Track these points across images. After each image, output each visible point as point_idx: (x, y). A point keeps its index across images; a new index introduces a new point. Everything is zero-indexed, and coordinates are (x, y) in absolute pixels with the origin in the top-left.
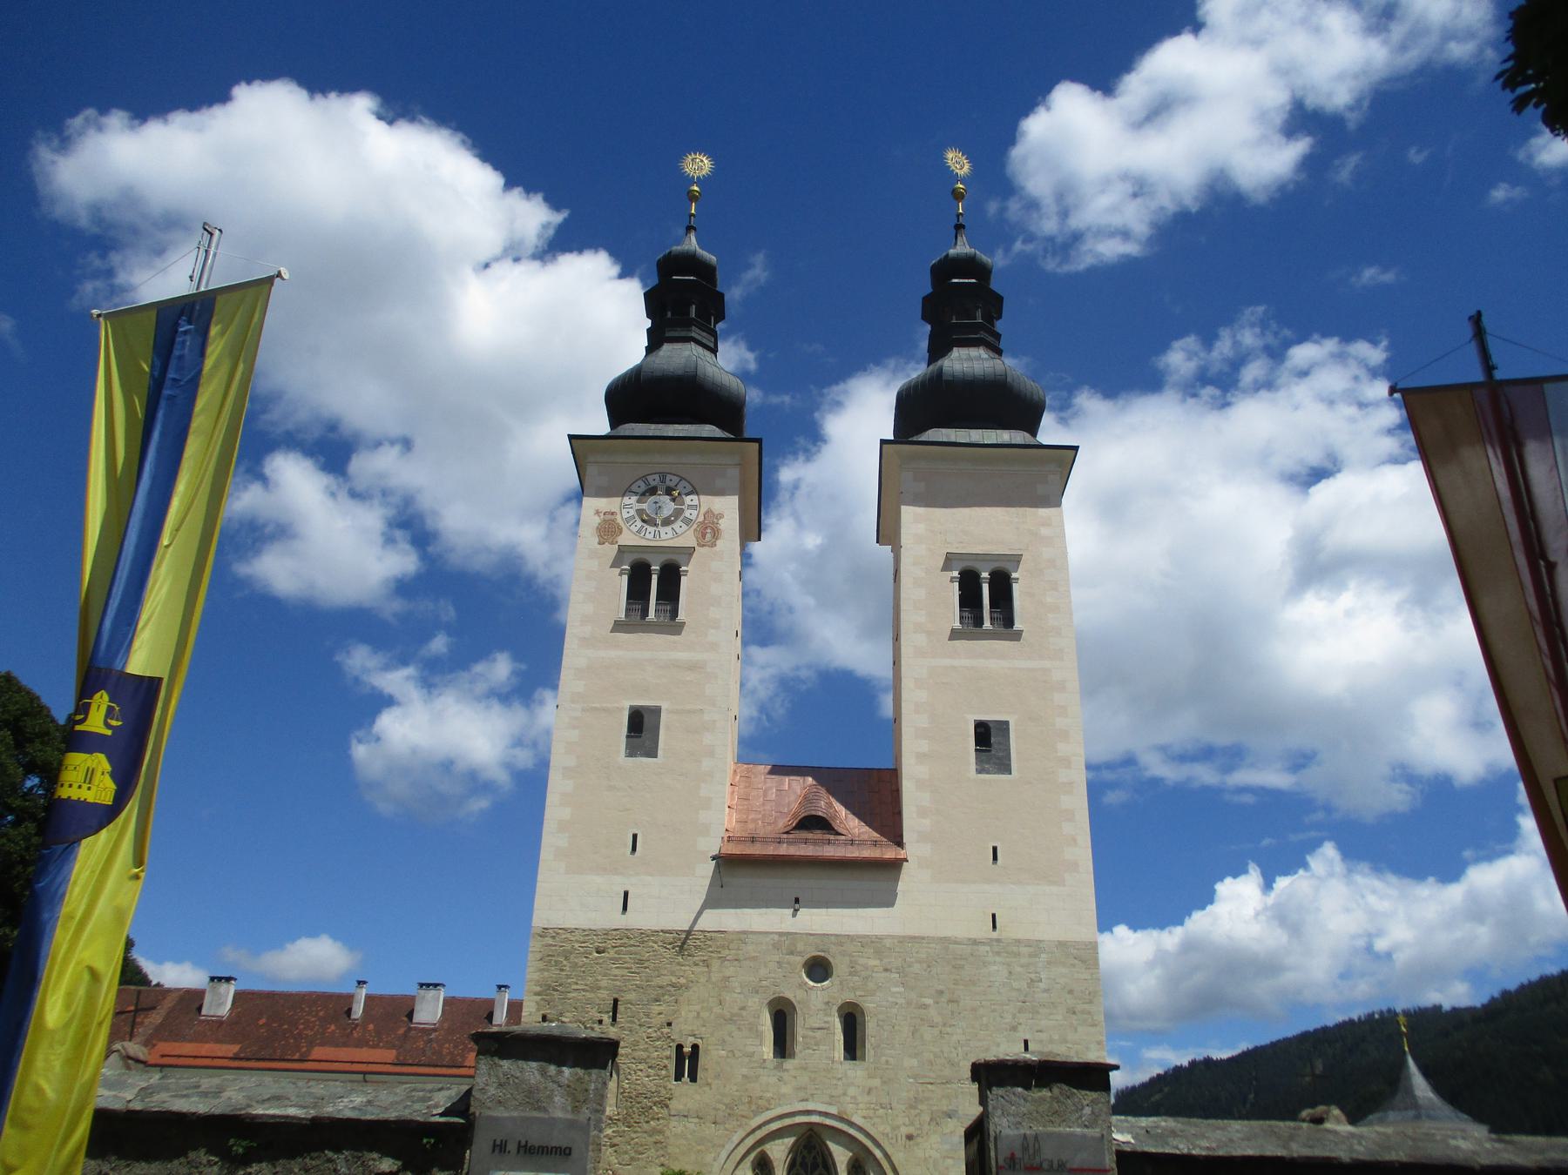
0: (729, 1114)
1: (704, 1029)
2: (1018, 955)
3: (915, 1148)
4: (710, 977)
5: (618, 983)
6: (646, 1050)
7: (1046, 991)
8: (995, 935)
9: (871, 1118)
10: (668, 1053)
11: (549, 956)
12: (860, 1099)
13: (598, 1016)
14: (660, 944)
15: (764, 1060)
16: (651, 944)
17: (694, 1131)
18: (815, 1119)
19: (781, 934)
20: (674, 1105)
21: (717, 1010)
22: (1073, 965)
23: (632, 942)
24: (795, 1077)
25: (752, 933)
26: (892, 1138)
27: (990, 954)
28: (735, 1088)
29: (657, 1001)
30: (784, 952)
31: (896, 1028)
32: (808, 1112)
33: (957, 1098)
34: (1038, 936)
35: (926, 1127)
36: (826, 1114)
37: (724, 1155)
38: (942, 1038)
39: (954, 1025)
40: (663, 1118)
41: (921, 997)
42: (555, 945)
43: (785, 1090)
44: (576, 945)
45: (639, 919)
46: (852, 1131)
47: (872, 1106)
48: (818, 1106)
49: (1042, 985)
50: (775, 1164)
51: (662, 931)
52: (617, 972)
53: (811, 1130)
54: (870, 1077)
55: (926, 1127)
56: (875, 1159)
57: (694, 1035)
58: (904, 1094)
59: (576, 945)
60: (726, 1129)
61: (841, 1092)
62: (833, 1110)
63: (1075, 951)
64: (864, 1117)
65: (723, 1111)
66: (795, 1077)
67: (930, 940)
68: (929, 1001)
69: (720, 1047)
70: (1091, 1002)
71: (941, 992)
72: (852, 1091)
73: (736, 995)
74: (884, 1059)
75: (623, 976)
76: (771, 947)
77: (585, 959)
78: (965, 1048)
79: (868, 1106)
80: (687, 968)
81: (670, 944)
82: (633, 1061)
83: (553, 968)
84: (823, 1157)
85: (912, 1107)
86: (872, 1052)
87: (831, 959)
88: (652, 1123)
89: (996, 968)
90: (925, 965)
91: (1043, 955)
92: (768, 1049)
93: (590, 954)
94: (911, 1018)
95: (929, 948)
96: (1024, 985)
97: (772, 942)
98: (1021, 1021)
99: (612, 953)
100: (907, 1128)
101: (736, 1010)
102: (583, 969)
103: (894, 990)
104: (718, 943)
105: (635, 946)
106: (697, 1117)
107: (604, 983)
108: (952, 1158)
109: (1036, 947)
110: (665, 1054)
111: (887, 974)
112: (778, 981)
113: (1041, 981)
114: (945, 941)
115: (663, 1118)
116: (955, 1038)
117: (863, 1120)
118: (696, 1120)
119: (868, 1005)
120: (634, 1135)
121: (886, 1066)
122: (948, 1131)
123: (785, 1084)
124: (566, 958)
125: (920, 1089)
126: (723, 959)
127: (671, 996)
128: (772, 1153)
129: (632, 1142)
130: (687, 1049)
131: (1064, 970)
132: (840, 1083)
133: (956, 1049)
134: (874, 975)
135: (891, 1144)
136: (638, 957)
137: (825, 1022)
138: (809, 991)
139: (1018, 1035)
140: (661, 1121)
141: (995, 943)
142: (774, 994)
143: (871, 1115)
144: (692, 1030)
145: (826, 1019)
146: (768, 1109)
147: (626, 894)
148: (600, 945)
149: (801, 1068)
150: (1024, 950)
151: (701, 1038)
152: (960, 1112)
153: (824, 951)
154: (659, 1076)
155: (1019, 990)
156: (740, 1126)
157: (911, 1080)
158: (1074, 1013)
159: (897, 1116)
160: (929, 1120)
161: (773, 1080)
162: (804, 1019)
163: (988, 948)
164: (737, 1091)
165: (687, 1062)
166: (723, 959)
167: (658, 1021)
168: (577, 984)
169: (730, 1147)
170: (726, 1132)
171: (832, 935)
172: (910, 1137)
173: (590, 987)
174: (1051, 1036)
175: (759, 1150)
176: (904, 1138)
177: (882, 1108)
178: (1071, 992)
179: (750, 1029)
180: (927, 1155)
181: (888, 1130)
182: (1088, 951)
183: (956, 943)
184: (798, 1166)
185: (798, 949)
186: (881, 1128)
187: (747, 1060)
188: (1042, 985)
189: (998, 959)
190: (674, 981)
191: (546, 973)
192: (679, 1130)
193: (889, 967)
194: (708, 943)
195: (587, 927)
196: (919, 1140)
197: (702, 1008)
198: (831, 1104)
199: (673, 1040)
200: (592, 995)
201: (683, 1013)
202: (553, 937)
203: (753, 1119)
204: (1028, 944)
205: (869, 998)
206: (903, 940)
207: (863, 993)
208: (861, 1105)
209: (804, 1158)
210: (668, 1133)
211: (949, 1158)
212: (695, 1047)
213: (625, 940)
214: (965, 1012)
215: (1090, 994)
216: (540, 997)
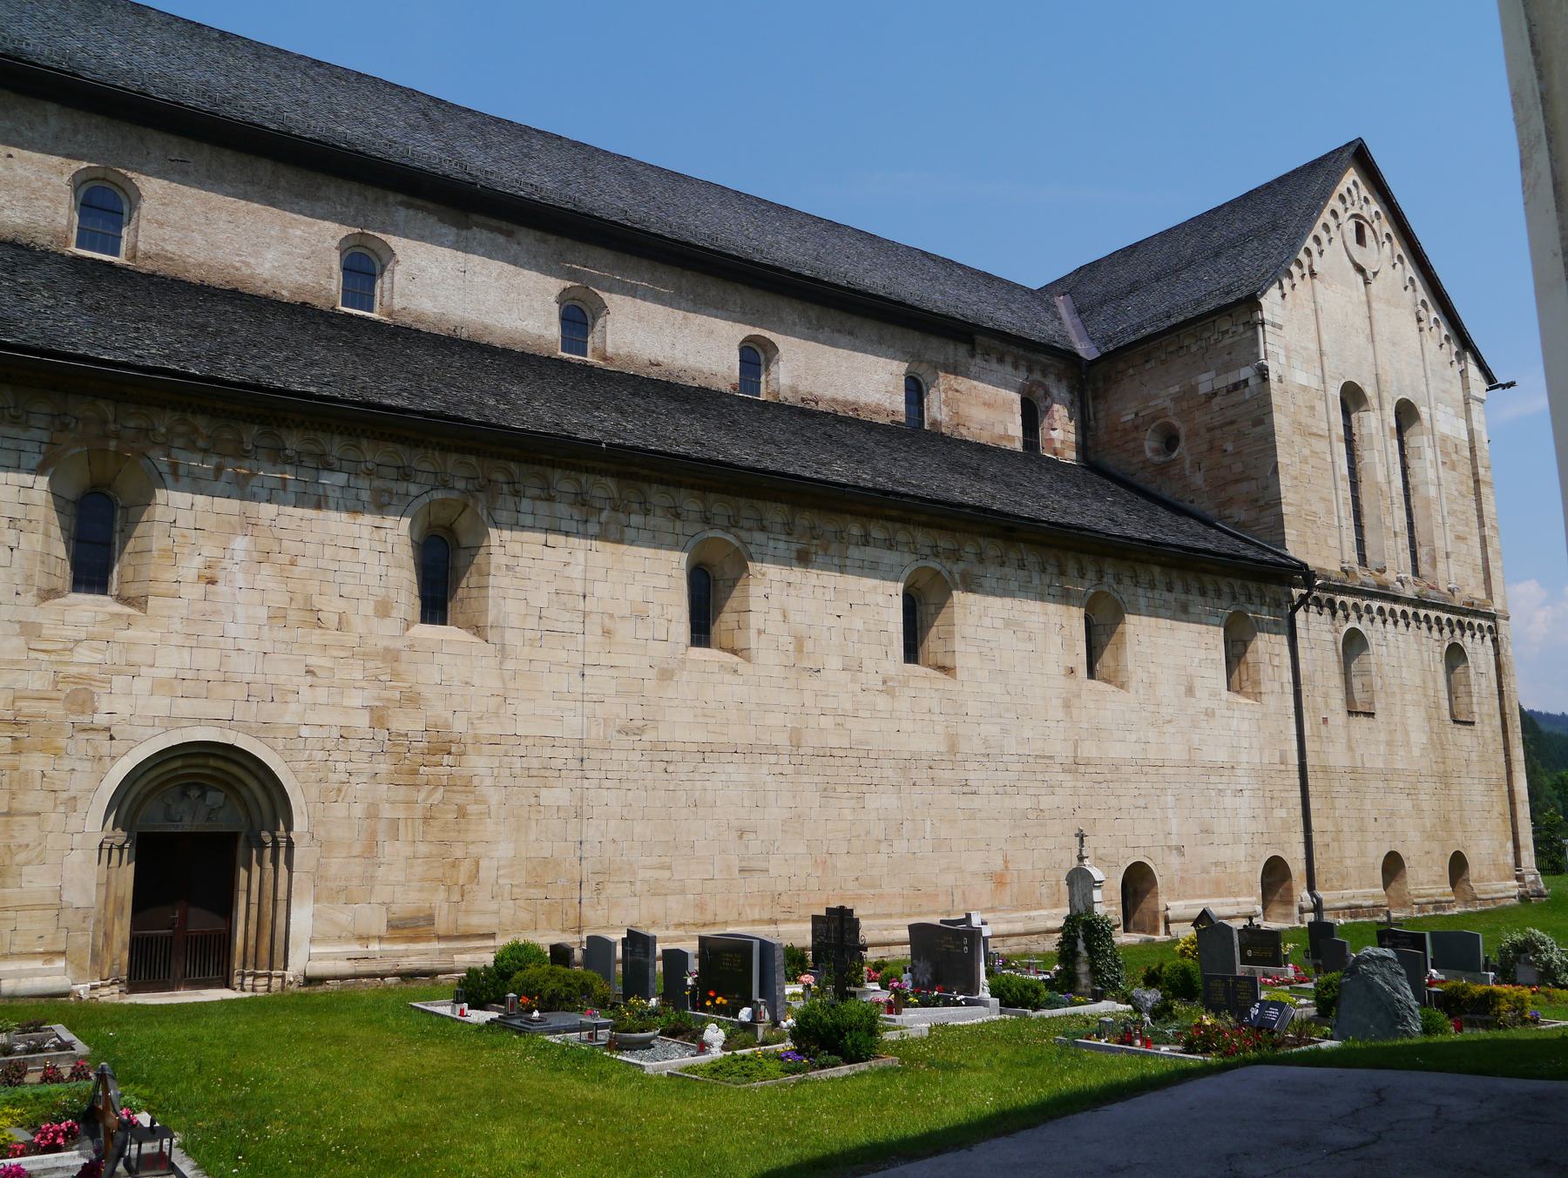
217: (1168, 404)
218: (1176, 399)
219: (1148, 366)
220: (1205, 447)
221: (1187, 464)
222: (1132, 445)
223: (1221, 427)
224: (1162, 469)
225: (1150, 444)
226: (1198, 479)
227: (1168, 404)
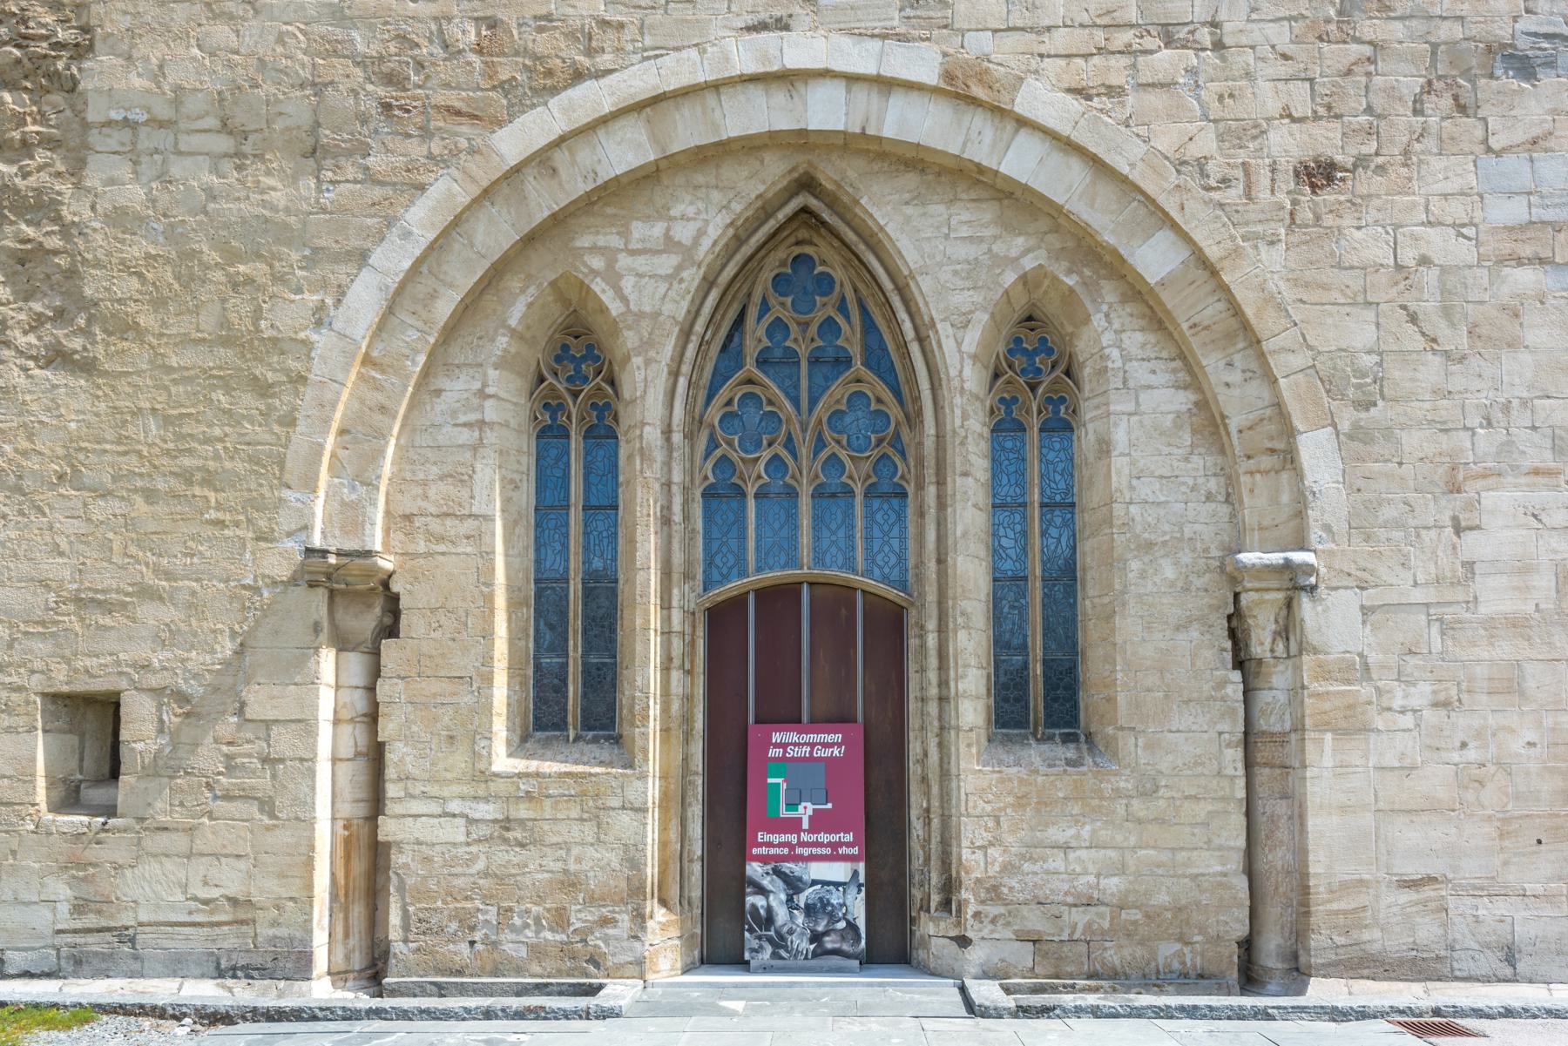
17: (211, 195)
26: (1225, 181)
32: (788, 78)
36: (885, 85)
47: (1122, 38)
50: (630, 339)
55: (1404, 119)
56: (1137, 292)
60: (370, 178)
62: (922, 65)
64: (1079, 92)
79: (1100, 36)
84: (869, 326)
106: (225, 127)
117: (1075, 104)
118: (224, 143)
122: (1520, 136)
128: (613, 278)
143: (1115, 80)
146: (578, 76)
170: (377, 193)
172: (1319, 174)
176: (1287, 182)
177: (1169, 42)
181: (1206, 143)
196: (1367, 182)
203: (500, 124)
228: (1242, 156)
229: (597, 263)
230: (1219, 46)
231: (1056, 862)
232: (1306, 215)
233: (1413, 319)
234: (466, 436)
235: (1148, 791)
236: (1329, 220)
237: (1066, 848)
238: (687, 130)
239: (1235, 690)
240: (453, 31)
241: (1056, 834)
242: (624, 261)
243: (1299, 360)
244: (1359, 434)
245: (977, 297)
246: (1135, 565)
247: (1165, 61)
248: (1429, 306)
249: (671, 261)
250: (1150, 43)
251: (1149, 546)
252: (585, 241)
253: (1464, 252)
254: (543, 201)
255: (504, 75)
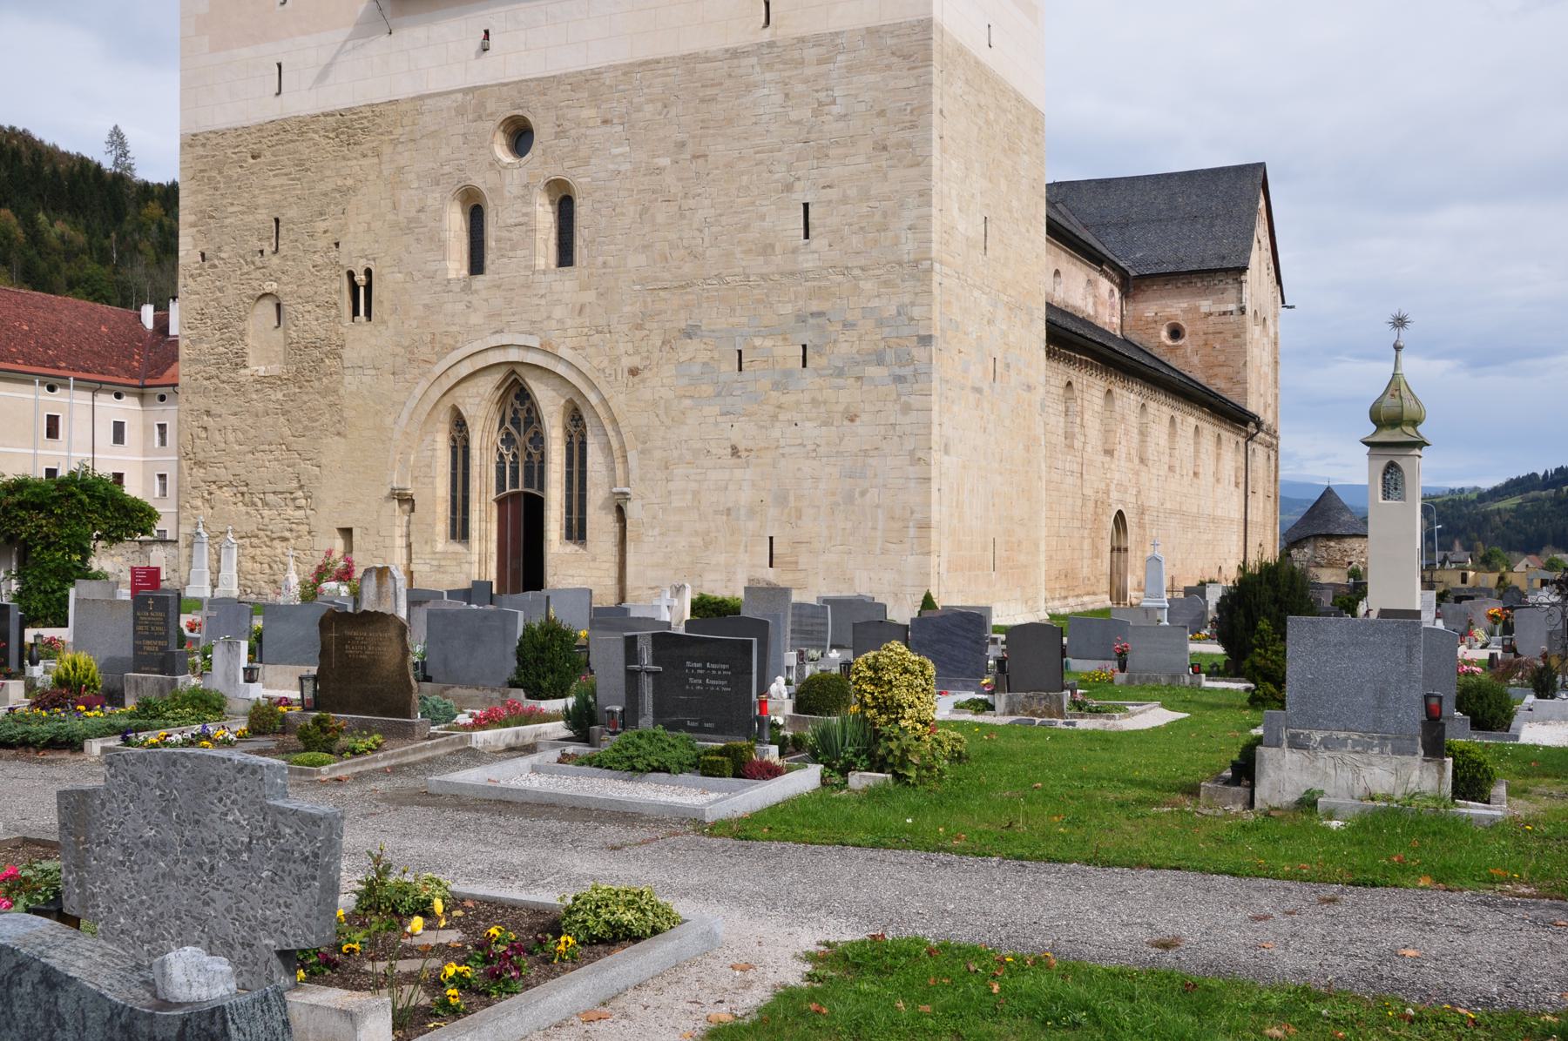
0: (409, 360)
1: (377, 245)
2: (802, 62)
3: (641, 386)
4: (381, 172)
5: (277, 197)
6: (312, 283)
7: (843, 117)
8: (766, 35)
9: (583, 348)
10: (336, 285)
11: (201, 171)
12: (569, 322)
13: (258, 245)
14: (322, 133)
15: (449, 281)
16: (311, 135)
18: (513, 355)
19: (465, 91)
20: (347, 353)
21: (390, 217)
22: (889, 67)
23: (289, 137)
24: (486, 300)
25: (430, 96)
27: (758, 69)
28: (415, 323)
29: (321, 214)
30: (470, 117)
31: (618, 210)
33: (700, 307)
34: (834, 26)
35: (656, 355)
36: (528, 348)
37: (405, 415)
38: (682, 217)
39: (699, 195)
40: (336, 373)
41: (654, 157)
42: (207, 156)
43: (475, 319)
44: (229, 152)
45: (301, 102)
46: (560, 369)
48: (517, 343)
49: (836, 109)
51: (323, 114)
52: (275, 182)
53: (513, 372)
54: (583, 288)
57: (366, 257)
58: (627, 309)
59: (229, 152)
61: (545, 315)
63: (895, 41)
64: (574, 349)
65: (402, 357)
66: (486, 300)
67: (670, 62)
68: (664, 162)
69: (396, 269)
70: (913, 127)
71: (683, 145)
72: (558, 312)
73: (413, 192)
74: (601, 259)
75: (282, 185)
76: (453, 113)
77: (239, 170)
78: (714, 229)
80: (354, 162)
81: (334, 130)
82: (300, 301)
83: (206, 188)
85: (639, 327)
86: (585, 251)
87: (531, 119)
88: (324, 380)
89: (766, 91)
90: (659, 105)
91: (839, 58)
92: (457, 264)
93: (246, 161)
94: (639, 191)
95: (668, 75)
96: (806, 113)
97: (455, 105)
98: (800, 173)
99: (268, 156)
100: (630, 358)
101: (413, 213)
102: (238, 184)
103: (616, 151)
104: (389, 119)
105: (292, 141)
107: (261, 201)
108: (691, 397)
109: (830, 44)
110: (333, 287)
111: (607, 128)
112: (463, 162)
113: (834, 102)
114: (690, 60)
115: (336, 373)
116: (701, 214)
118: (373, 372)
119: (580, 183)
120: (305, 398)
121: (604, 270)
123: (475, 310)
124: (220, 173)
125: (649, 300)
126: (395, 143)
127: (337, 204)
129: (304, 407)
130: (360, 278)
131: (873, 78)
132: (543, 302)
133: (701, 231)
134: (589, 132)
135: (608, 382)
136: (297, 156)
137: (525, 215)
138: (502, 171)
139: (794, 196)
140: (335, 377)
141: (765, 51)
142: (459, 182)
144: (363, 250)
145: (524, 210)
146: (453, 349)
147: (280, 66)
148: (255, 147)
149: (494, 286)
150: (811, 53)
151: (374, 260)
152: (703, 328)
153: (521, 108)
154: (328, 317)
155: (798, 122)
156: (423, 375)
157: (638, 287)
158: (885, 148)
159: (617, 342)
160: (660, 343)
161: (461, 306)
162: (497, 213)
163: (754, 60)
164: (418, 327)
165: (361, 294)
166: (395, 143)
167: (323, 243)
168: (232, 204)
169: (412, 404)
171: (531, 80)
172: (634, 372)
173: (248, 207)
174: (844, 191)
175: (448, 401)
176: (626, 370)
178: (881, 113)
179: (431, 239)
180: (656, 397)
182: (914, 37)
183: (708, 60)
184: (507, 424)
185: (489, 111)
186: (595, 363)
187: (428, 282)
188: (836, 109)
189: (768, 76)
190: (339, 183)
191: (200, 197)
192: (353, 388)
193: (609, 117)
194: (378, 120)
195: (238, 125)
196: (646, 374)
197: (374, 215)
198: (531, 334)
199: (342, 267)
200: (251, 218)
201: (352, 229)
202: (204, 145)
204: (818, 41)
205: (580, 171)
206: (628, 70)
207: (574, 164)
208: (570, 332)
209: (515, 411)
210: (342, 392)
211: (685, 396)
212: (368, 273)
213: (282, 135)
214: (715, 172)
215: (912, 112)
216: (195, 229)
217: (1179, 312)
218: (1184, 311)
219: (1167, 287)
220: (1202, 343)
221: (1189, 351)
222: (1151, 331)
223: (1214, 333)
224: (1172, 349)
225: (1164, 334)
226: (1195, 360)
227: (1179, 312)
228: (615, 367)
229: (460, 400)
230: (610, 332)
231: (570, 580)
232: (630, 384)
233: (657, 416)
234: (430, 453)
235: (594, 560)
236: (636, 386)
237: (573, 576)
238: (480, 362)
239: (617, 530)
240: (424, 338)
241: (570, 572)
242: (467, 400)
243: (627, 429)
244: (642, 452)
245: (555, 408)
246: (592, 491)
247: (596, 338)
248: (661, 412)
249: (479, 399)
250: (592, 332)
251: (596, 484)
252: (457, 394)
253: (671, 395)
254: (447, 383)
255: (436, 349)
